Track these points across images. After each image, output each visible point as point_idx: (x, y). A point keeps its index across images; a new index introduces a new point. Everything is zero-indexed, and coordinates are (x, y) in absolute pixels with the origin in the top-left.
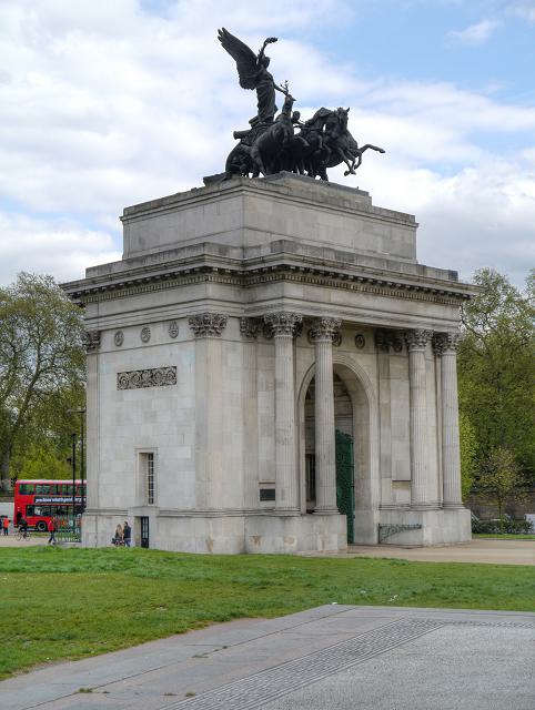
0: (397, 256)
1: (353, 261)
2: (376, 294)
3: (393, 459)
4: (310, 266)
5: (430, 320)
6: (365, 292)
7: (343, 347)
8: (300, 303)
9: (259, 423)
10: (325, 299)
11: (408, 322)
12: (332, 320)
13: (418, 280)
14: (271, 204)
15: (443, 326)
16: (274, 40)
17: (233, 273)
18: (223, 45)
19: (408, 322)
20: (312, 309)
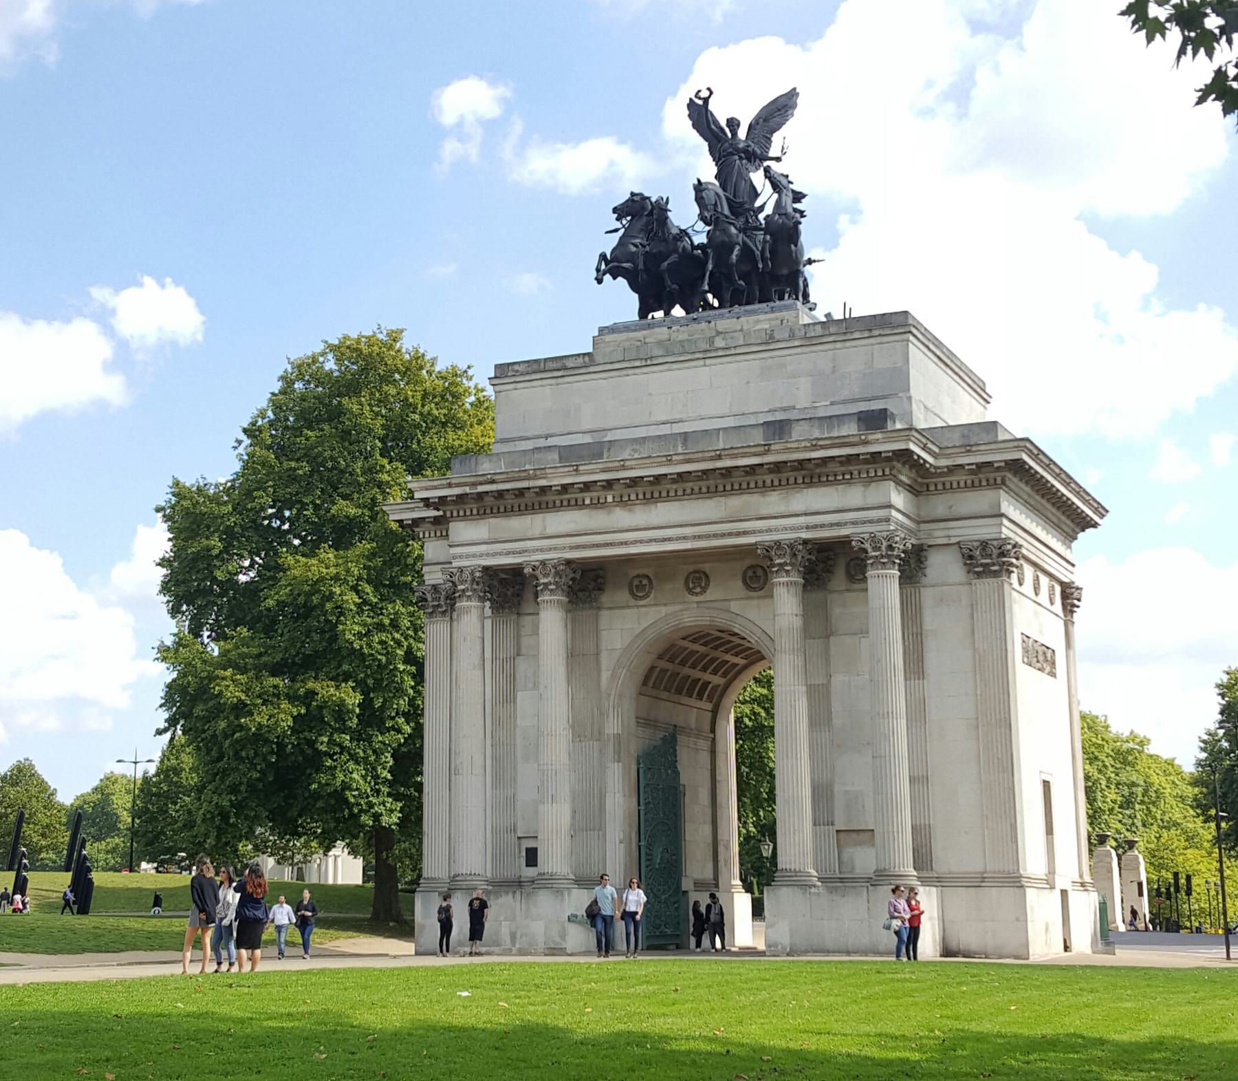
0: (844, 402)
1: (600, 455)
2: (650, 499)
3: (837, 788)
4: (467, 490)
5: (802, 520)
6: (621, 502)
7: (711, 594)
8: (483, 548)
9: (519, 741)
10: (537, 531)
11: (738, 534)
12: (543, 563)
13: (719, 457)
14: (548, 390)
15: (838, 524)
16: (699, 91)
17: (435, 518)
18: (694, 126)
19: (745, 533)
20: (508, 553)
